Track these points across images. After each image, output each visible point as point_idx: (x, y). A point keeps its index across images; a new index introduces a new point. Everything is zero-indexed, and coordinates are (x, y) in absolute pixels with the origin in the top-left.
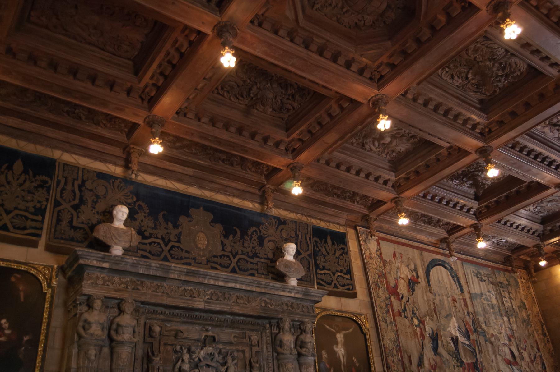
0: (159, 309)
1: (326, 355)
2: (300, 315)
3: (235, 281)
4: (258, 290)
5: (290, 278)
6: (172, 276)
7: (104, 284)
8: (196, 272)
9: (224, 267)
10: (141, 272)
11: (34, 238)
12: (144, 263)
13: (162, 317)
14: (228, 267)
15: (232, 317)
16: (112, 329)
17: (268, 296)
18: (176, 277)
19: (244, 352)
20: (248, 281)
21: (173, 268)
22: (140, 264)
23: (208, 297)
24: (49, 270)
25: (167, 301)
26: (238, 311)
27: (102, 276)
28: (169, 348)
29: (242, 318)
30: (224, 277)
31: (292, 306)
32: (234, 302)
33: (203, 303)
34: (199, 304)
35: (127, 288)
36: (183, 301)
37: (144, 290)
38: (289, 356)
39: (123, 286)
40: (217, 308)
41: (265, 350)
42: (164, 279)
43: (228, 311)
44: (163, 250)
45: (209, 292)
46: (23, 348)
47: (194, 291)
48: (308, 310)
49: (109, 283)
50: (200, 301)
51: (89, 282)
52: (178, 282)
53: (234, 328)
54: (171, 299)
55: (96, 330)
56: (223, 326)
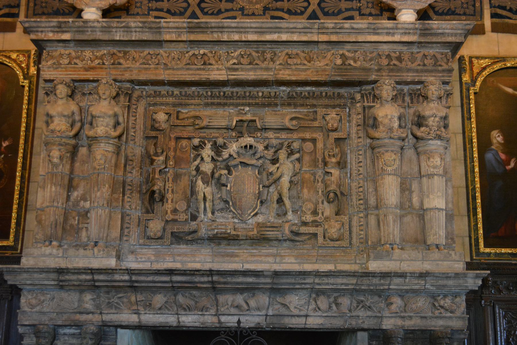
0: (163, 90)
1: (500, 139)
2: (417, 71)
3: (278, 30)
4: (324, 38)
5: (400, 10)
6: (167, 37)
7: (70, 63)
8: (202, 25)
9: (296, 14)
10: (118, 38)
11: (9, 20)
12: (119, 25)
13: (171, 100)
14: (302, 13)
15: (288, 89)
16: (83, 122)
17: (348, 47)
18: (174, 37)
19: (314, 141)
20: (300, 26)
21: (164, 25)
22: (113, 27)
23: (235, 61)
24: (24, 55)
25: (164, 75)
26: (288, 78)
27: (67, 52)
28: (184, 143)
29: (308, 88)
30: (254, 25)
31: (399, 59)
32: (280, 64)
33: (224, 72)
34: (218, 74)
35: (104, 64)
36: (191, 72)
37: (126, 64)
38: (386, 141)
39: (97, 62)
40: (251, 76)
41: (354, 135)
42: (159, 43)
43: (271, 78)
44: (189, 5)
45: (236, 54)
46: (3, 156)
47: (209, 55)
48: (436, 60)
49: (77, 61)
50: (218, 69)
51: (49, 63)
52: (182, 45)
53: (296, 106)
54: (171, 72)
55: (60, 125)
56: (276, 105)
